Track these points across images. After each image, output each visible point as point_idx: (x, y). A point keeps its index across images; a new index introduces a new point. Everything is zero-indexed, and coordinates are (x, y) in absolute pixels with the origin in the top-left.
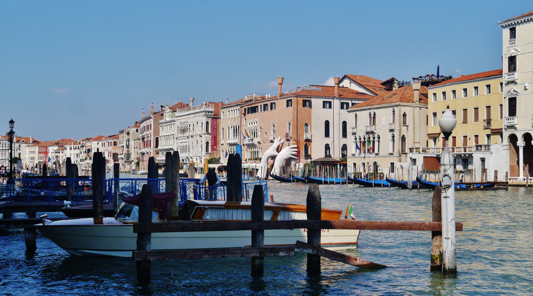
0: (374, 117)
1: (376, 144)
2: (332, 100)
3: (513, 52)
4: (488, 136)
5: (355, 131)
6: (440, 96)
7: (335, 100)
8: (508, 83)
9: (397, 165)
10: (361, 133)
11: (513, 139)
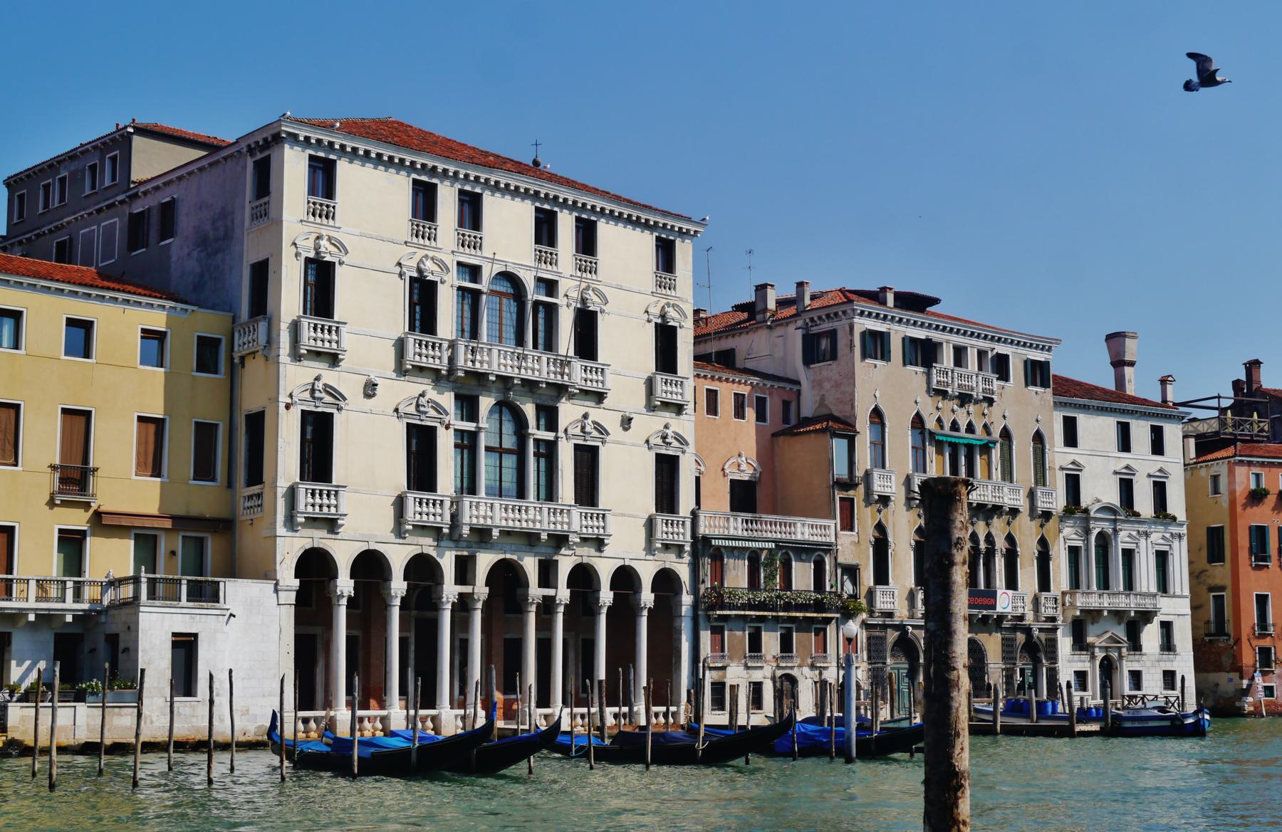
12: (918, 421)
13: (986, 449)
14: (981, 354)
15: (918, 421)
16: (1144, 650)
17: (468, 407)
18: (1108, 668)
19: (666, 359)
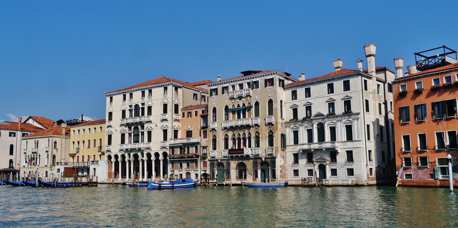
0: (38, 143)
1: (38, 160)
2: (16, 132)
3: (111, 110)
4: (100, 156)
5: (25, 151)
6: (77, 132)
7: (18, 132)
8: (108, 127)
9: (49, 172)
10: (29, 153)
11: (110, 157)
12: (227, 108)
13: (249, 108)
14: (249, 84)
15: (227, 108)
16: (338, 161)
17: (130, 128)
18: (322, 168)
19: (165, 111)
